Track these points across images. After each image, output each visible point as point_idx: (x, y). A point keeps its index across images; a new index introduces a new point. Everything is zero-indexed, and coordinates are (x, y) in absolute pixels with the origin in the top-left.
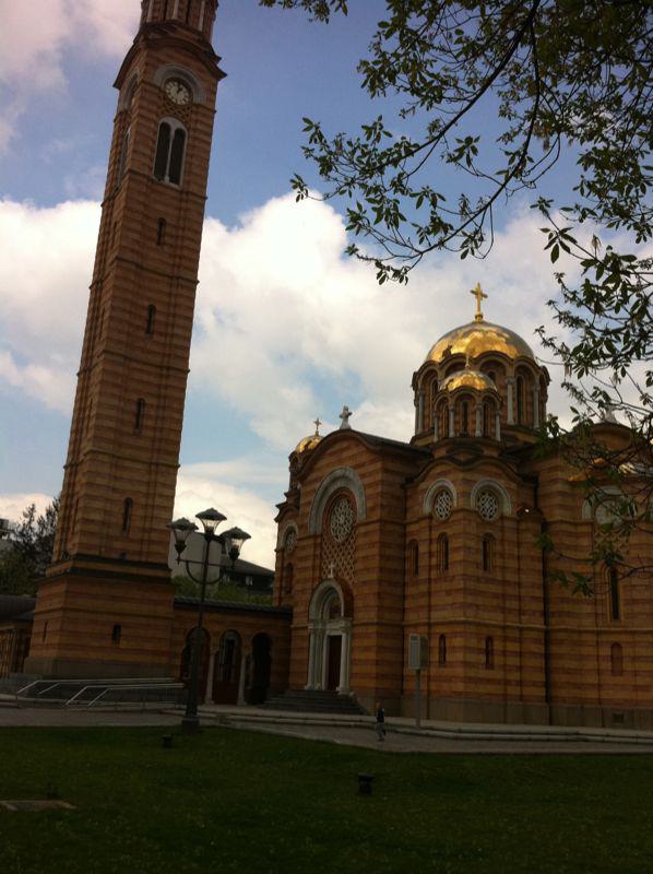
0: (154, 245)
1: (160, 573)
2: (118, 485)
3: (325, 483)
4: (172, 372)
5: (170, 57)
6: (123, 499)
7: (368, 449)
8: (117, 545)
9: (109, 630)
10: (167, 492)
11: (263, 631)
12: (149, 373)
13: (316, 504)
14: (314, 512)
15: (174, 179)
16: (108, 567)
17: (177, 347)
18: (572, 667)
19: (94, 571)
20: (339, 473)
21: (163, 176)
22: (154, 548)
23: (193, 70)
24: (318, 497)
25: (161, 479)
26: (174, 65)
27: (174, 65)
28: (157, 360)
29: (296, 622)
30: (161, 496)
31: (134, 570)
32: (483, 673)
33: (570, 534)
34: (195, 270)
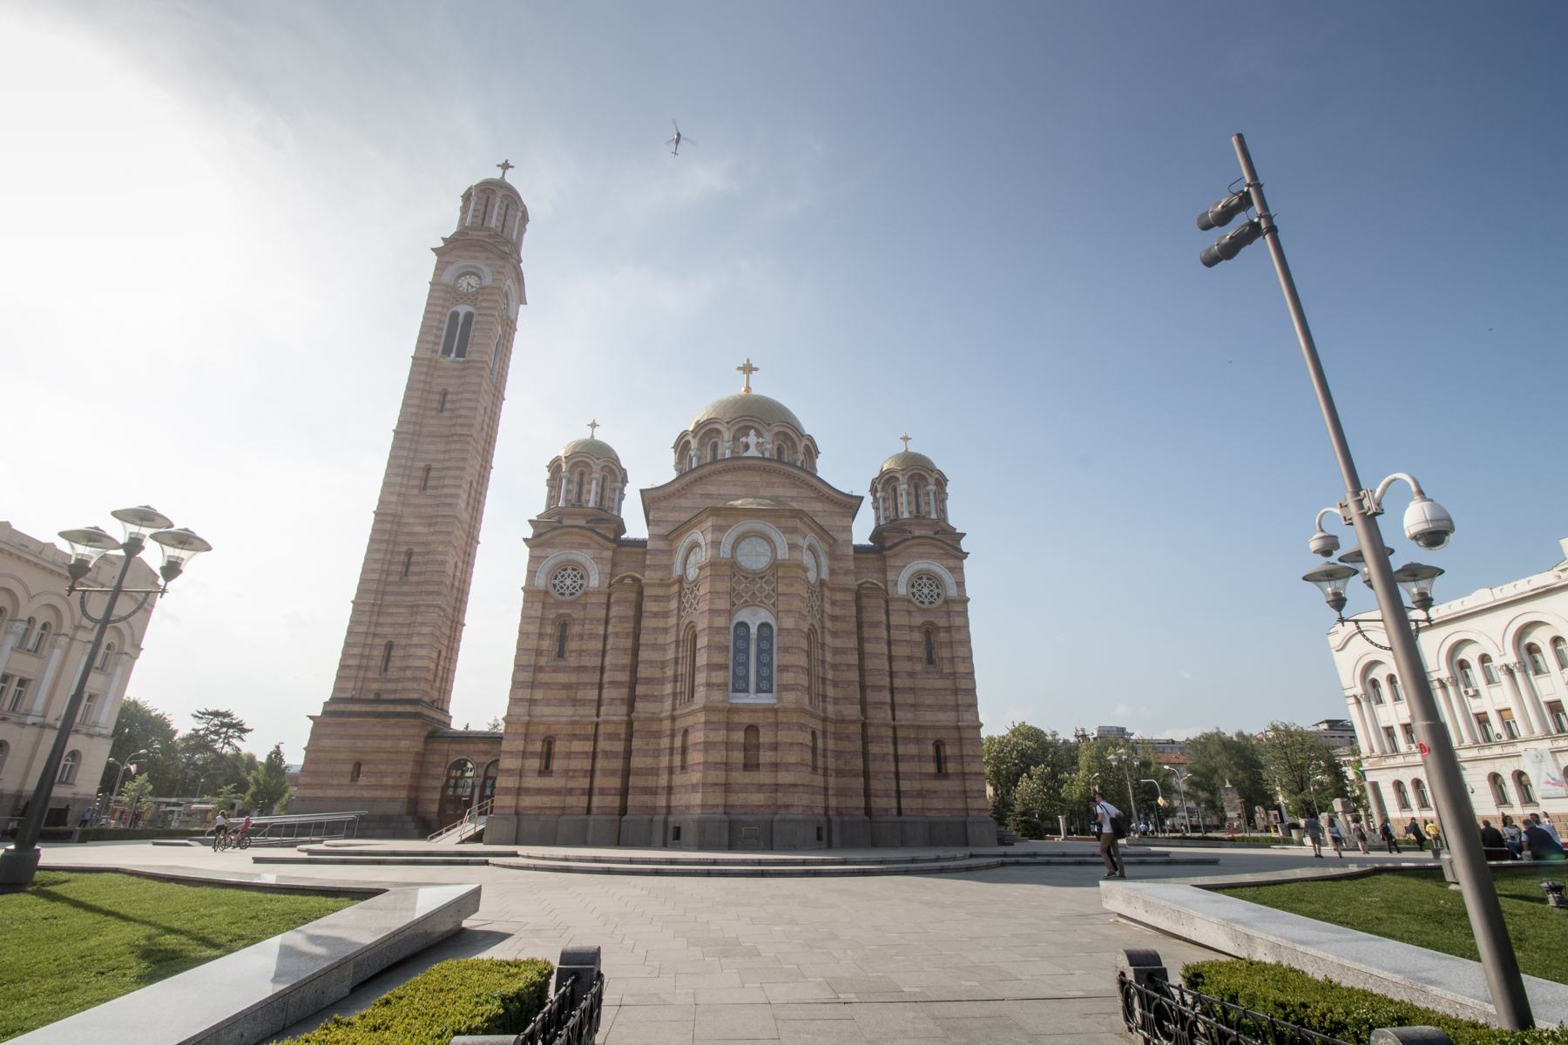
0: (433, 413)
2: (380, 630)
6: (384, 643)
8: (375, 686)
9: (349, 768)
15: (461, 354)
18: (642, 766)
27: (462, 263)
30: (418, 634)
32: (532, 782)
33: (657, 599)
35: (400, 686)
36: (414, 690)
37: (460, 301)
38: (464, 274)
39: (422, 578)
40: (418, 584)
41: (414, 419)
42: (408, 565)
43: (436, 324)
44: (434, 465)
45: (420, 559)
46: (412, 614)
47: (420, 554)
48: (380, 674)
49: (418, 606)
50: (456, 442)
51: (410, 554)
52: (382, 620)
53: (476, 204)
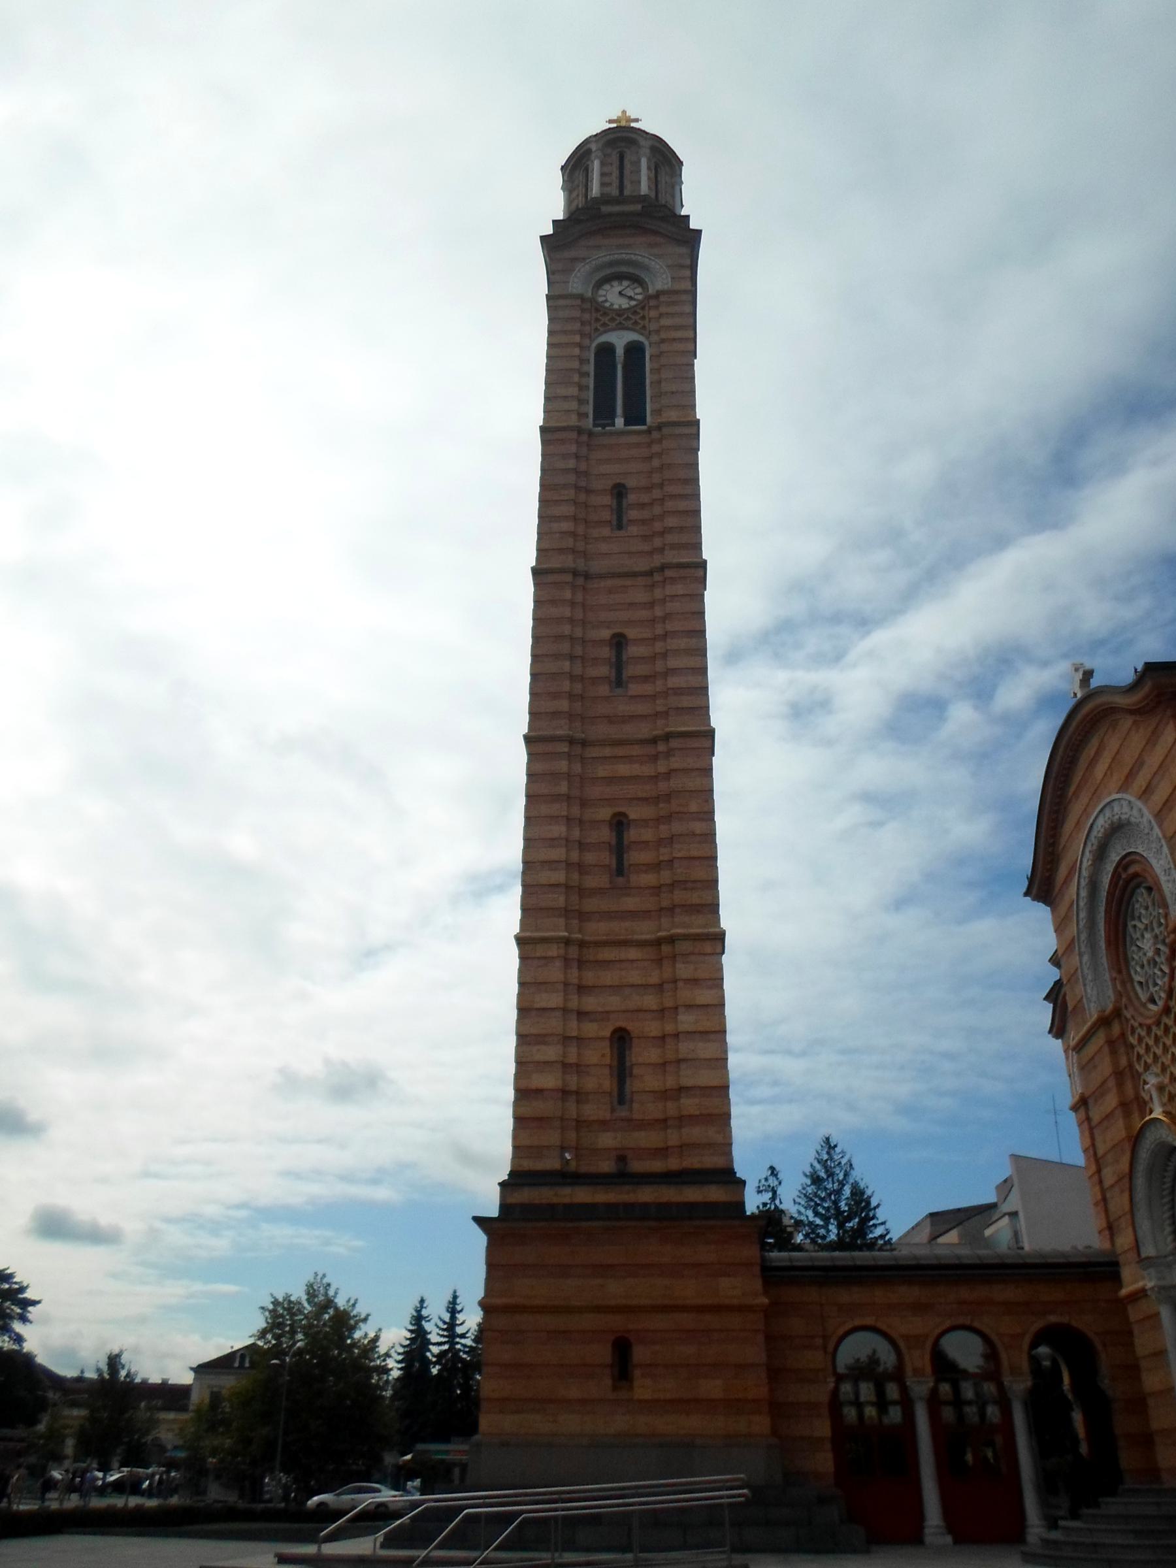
0: (606, 531)
1: (715, 1194)
2: (591, 1003)
3: (1085, 873)
4: (674, 743)
5: (598, 247)
7: (1131, 712)
8: (607, 1140)
9: (603, 1353)
10: (704, 996)
11: (1053, 1319)
12: (629, 759)
13: (1083, 936)
14: (1086, 958)
16: (582, 1195)
17: (678, 691)
19: (552, 1207)
20: (1102, 824)
21: (612, 416)
22: (695, 1133)
23: (639, 251)
24: (1083, 915)
25: (683, 970)
26: (602, 256)
27: (602, 256)
28: (644, 730)
29: (1133, 1280)
30: (690, 1007)
31: (646, 1195)
34: (696, 546)
35: (673, 1137)
36: (711, 1145)
37: (613, 325)
38: (608, 280)
39: (666, 876)
40: (657, 890)
41: (570, 542)
42: (619, 850)
43: (576, 364)
44: (631, 633)
45: (647, 834)
46: (659, 961)
47: (644, 823)
48: (613, 1110)
49: (672, 940)
50: (673, 580)
51: (619, 823)
52: (590, 977)
53: (602, 164)
